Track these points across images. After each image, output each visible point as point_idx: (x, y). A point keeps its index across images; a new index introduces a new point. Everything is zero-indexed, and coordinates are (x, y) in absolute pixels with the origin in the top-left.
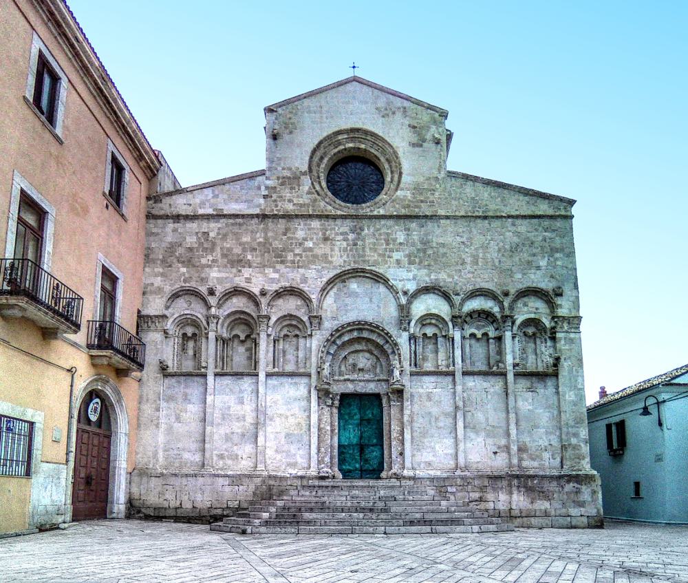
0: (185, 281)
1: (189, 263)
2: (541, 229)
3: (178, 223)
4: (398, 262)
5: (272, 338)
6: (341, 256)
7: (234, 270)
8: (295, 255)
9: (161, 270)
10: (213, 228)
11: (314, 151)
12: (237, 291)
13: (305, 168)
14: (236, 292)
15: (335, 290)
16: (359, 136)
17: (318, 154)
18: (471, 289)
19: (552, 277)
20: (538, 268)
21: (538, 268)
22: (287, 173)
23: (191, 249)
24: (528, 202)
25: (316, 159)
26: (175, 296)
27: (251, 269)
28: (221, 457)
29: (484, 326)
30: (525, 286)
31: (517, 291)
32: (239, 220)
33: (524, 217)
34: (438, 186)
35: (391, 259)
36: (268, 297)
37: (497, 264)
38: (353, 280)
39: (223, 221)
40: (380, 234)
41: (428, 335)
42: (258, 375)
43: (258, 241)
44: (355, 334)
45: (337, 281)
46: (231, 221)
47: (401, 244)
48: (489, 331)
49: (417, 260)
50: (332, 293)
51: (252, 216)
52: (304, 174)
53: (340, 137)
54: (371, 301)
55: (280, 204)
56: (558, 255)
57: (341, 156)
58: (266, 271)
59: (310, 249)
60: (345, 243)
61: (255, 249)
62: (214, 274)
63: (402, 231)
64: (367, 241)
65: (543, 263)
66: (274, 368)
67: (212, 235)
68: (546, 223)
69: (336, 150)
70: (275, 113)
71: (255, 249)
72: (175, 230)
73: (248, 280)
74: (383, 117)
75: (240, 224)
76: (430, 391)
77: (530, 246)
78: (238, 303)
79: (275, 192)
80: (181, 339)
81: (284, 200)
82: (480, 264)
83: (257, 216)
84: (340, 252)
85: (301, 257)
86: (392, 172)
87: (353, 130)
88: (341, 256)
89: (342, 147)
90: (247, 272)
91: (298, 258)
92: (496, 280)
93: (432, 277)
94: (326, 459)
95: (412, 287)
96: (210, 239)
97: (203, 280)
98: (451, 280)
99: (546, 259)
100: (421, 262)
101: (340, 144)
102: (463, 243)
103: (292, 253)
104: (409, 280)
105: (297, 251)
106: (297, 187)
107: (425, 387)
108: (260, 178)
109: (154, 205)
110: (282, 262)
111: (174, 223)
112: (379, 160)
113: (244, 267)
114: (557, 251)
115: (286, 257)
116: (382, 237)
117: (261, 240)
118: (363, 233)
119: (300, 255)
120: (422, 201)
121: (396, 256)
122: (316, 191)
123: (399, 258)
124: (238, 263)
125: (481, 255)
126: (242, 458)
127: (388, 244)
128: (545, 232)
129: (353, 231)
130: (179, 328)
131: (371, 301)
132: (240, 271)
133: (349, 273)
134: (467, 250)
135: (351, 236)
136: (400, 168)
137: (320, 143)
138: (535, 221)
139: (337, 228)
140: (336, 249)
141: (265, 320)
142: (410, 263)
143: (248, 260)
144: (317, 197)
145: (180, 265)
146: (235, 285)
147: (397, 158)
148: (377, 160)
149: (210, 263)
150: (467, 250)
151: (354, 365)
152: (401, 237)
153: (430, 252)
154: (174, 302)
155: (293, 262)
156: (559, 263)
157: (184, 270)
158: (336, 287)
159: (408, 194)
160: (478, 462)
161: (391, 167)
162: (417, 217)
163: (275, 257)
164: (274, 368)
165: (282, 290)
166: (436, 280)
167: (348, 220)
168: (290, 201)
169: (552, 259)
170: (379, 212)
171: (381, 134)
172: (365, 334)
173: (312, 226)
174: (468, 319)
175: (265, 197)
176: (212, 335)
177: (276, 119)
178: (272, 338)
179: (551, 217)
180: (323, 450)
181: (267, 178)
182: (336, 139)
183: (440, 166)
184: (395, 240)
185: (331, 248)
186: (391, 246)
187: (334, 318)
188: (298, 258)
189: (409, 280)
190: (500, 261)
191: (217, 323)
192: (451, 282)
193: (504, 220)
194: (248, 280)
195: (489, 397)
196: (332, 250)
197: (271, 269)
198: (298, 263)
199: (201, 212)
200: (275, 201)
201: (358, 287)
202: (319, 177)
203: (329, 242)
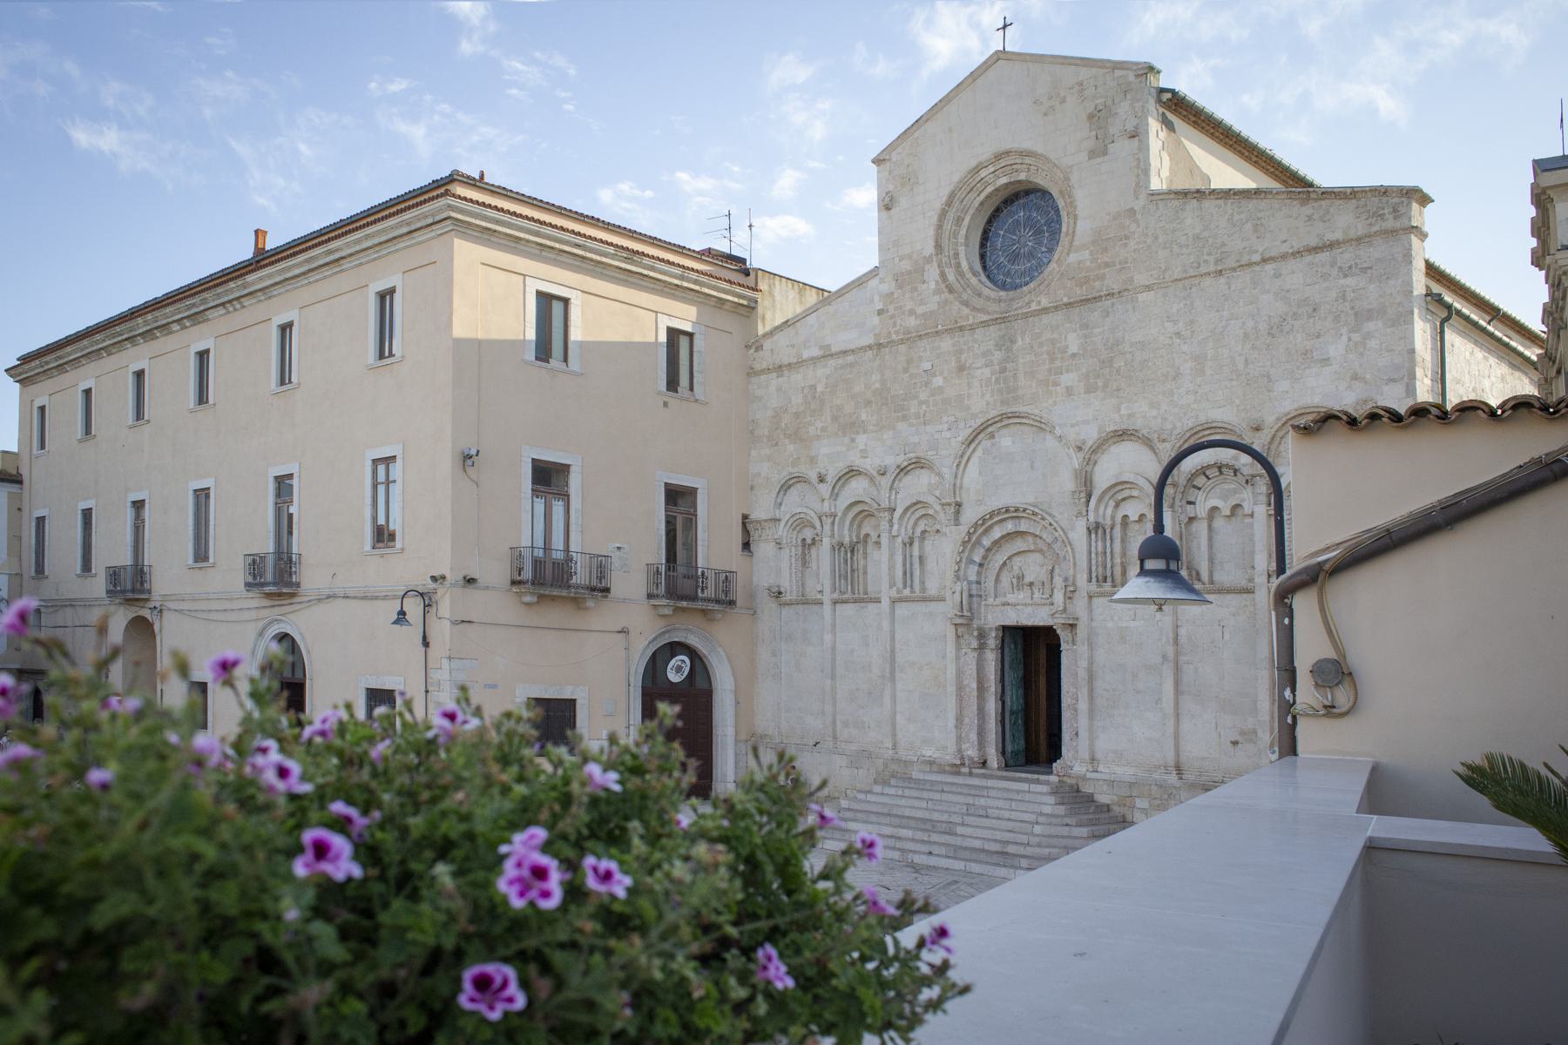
0: (794, 464)
1: (797, 436)
2: (1335, 271)
3: (782, 376)
4: (1069, 391)
5: (899, 540)
6: (983, 395)
7: (847, 440)
8: (921, 403)
9: (768, 451)
10: (819, 375)
11: (943, 215)
12: (853, 470)
13: (929, 249)
14: (852, 473)
15: (979, 452)
16: (1012, 162)
17: (951, 215)
18: (1190, 425)
19: (1355, 377)
20: (1326, 361)
21: (1326, 361)
22: (906, 265)
23: (797, 415)
24: (1310, 218)
25: (948, 226)
26: (786, 487)
27: (866, 436)
28: (846, 724)
29: (1235, 492)
30: (1296, 406)
31: (1278, 419)
32: (850, 358)
33: (1297, 254)
34: (1133, 227)
35: (1058, 388)
36: (889, 477)
37: (1241, 366)
38: (1005, 431)
39: (832, 362)
40: (1041, 345)
41: (1132, 519)
42: (880, 602)
43: (873, 388)
44: (1010, 526)
45: (980, 437)
46: (840, 361)
47: (1074, 355)
48: (1243, 500)
49: (1100, 384)
50: (974, 459)
51: (864, 349)
52: (928, 260)
53: (983, 173)
54: (1032, 467)
55: (899, 322)
56: (1371, 326)
57: (996, 201)
58: (885, 437)
59: (940, 390)
60: (987, 371)
61: (869, 403)
62: (824, 449)
63: (1075, 331)
64: (1021, 361)
65: (1336, 350)
66: (905, 587)
67: (819, 389)
68: (1346, 256)
70: (888, 164)
71: (869, 403)
72: (779, 389)
73: (864, 454)
75: (851, 365)
76: (1125, 624)
77: (1310, 317)
78: (857, 488)
79: (891, 302)
80: (800, 548)
81: (903, 313)
82: (1208, 372)
83: (870, 347)
84: (981, 387)
85: (928, 407)
87: (998, 157)
88: (983, 395)
89: (989, 189)
90: (862, 440)
91: (924, 407)
92: (1237, 402)
93: (1123, 411)
94: (971, 736)
95: (1091, 435)
96: (817, 395)
97: (813, 460)
98: (1154, 413)
99: (1345, 338)
100: (1105, 386)
102: (1178, 334)
103: (916, 402)
104: (1086, 422)
105: (923, 396)
107: (1116, 618)
108: (874, 283)
109: (755, 354)
110: (904, 418)
111: (778, 377)
113: (858, 433)
114: (1369, 315)
115: (908, 410)
116: (1045, 349)
117: (877, 385)
118: (1015, 347)
119: (925, 402)
120: (1107, 265)
121: (1068, 379)
123: (1070, 384)
124: (851, 427)
125: (1210, 353)
126: (869, 727)
127: (1052, 360)
128: (1346, 276)
129: (999, 347)
130: (795, 532)
131: (1032, 467)
132: (853, 440)
133: (996, 422)
134: (1185, 348)
135: (998, 355)
137: (952, 196)
138: (1324, 256)
140: (976, 383)
141: (886, 514)
142: (1088, 391)
143: (863, 421)
145: (787, 441)
146: (849, 464)
149: (819, 433)
150: (1185, 348)
151: (1020, 578)
152: (1073, 343)
153: (1119, 363)
154: (787, 494)
155: (917, 416)
156: (1373, 343)
157: (791, 448)
158: (980, 448)
159: (1086, 254)
160: (1203, 759)
162: (1097, 299)
163: (895, 412)
164: (905, 587)
165: (906, 463)
166: (1130, 416)
167: (992, 328)
168: (912, 312)
169: (1356, 337)
170: (1039, 303)
172: (1023, 526)
174: (1200, 481)
175: (880, 312)
176: (826, 541)
177: (890, 173)
178: (899, 540)
179: (1359, 240)
180: (966, 720)
181: (882, 281)
183: (1138, 184)
184: (1064, 350)
185: (968, 383)
186: (1058, 363)
187: (980, 502)
188: (924, 407)
189: (1086, 422)
190: (1246, 360)
191: (833, 523)
192: (1155, 417)
193: (1257, 268)
194: (864, 454)
195: (1227, 636)
196: (969, 385)
197: (891, 433)
198: (924, 415)
199: (806, 354)
200: (892, 317)
201: (1013, 442)
202: (956, 255)
203: (965, 373)
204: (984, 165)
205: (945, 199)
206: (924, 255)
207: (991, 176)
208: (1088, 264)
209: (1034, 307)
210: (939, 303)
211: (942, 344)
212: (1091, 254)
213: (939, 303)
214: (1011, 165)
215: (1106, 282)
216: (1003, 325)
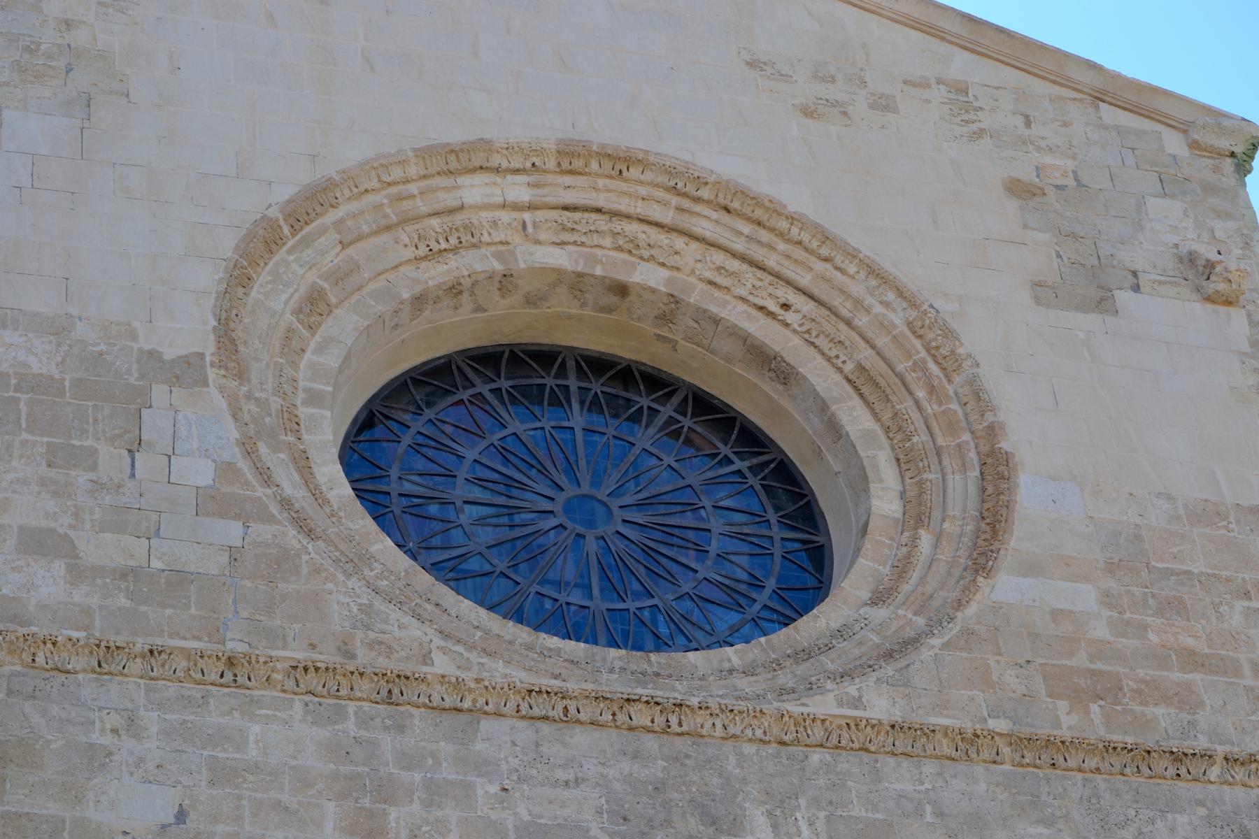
16: (623, 205)
53: (474, 189)
69: (437, 274)
74: (808, 112)
86: (905, 461)
101: (469, 239)
106: (110, 458)
112: (784, 374)
122: (286, 504)
136: (993, 431)
139: (486, 788)
144: (293, 537)
147: (951, 363)
148: (769, 387)
161: (896, 430)
167: (580, 738)
170: (857, 703)
171: (796, 199)
173: (252, 753)
182: (447, 200)
204: (496, 160)
205: (284, 193)
206: (145, 343)
207: (505, 216)
208: (1100, 631)
209: (825, 705)
210: (234, 555)
211: (256, 729)
212: (1107, 598)
213: (234, 555)
214: (615, 214)
215: (1201, 717)
216: (650, 743)
